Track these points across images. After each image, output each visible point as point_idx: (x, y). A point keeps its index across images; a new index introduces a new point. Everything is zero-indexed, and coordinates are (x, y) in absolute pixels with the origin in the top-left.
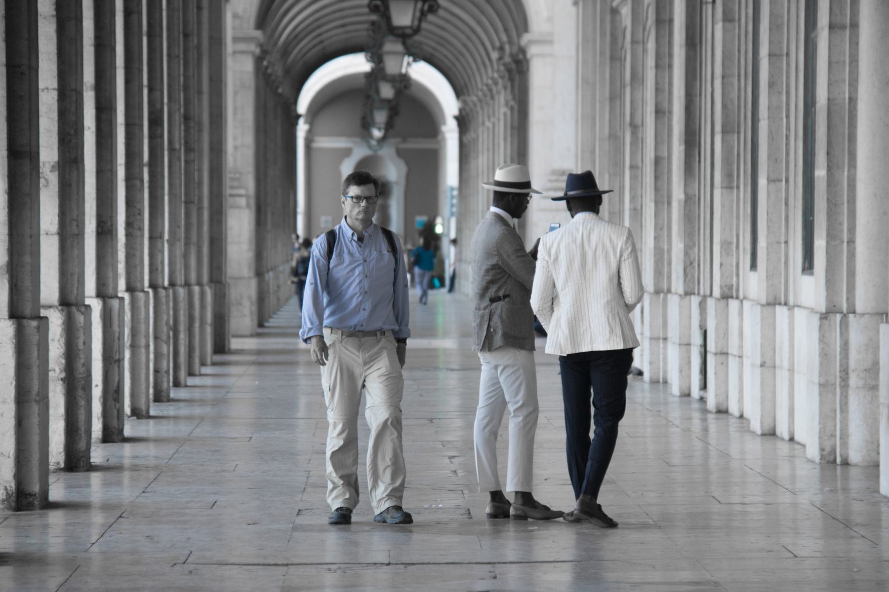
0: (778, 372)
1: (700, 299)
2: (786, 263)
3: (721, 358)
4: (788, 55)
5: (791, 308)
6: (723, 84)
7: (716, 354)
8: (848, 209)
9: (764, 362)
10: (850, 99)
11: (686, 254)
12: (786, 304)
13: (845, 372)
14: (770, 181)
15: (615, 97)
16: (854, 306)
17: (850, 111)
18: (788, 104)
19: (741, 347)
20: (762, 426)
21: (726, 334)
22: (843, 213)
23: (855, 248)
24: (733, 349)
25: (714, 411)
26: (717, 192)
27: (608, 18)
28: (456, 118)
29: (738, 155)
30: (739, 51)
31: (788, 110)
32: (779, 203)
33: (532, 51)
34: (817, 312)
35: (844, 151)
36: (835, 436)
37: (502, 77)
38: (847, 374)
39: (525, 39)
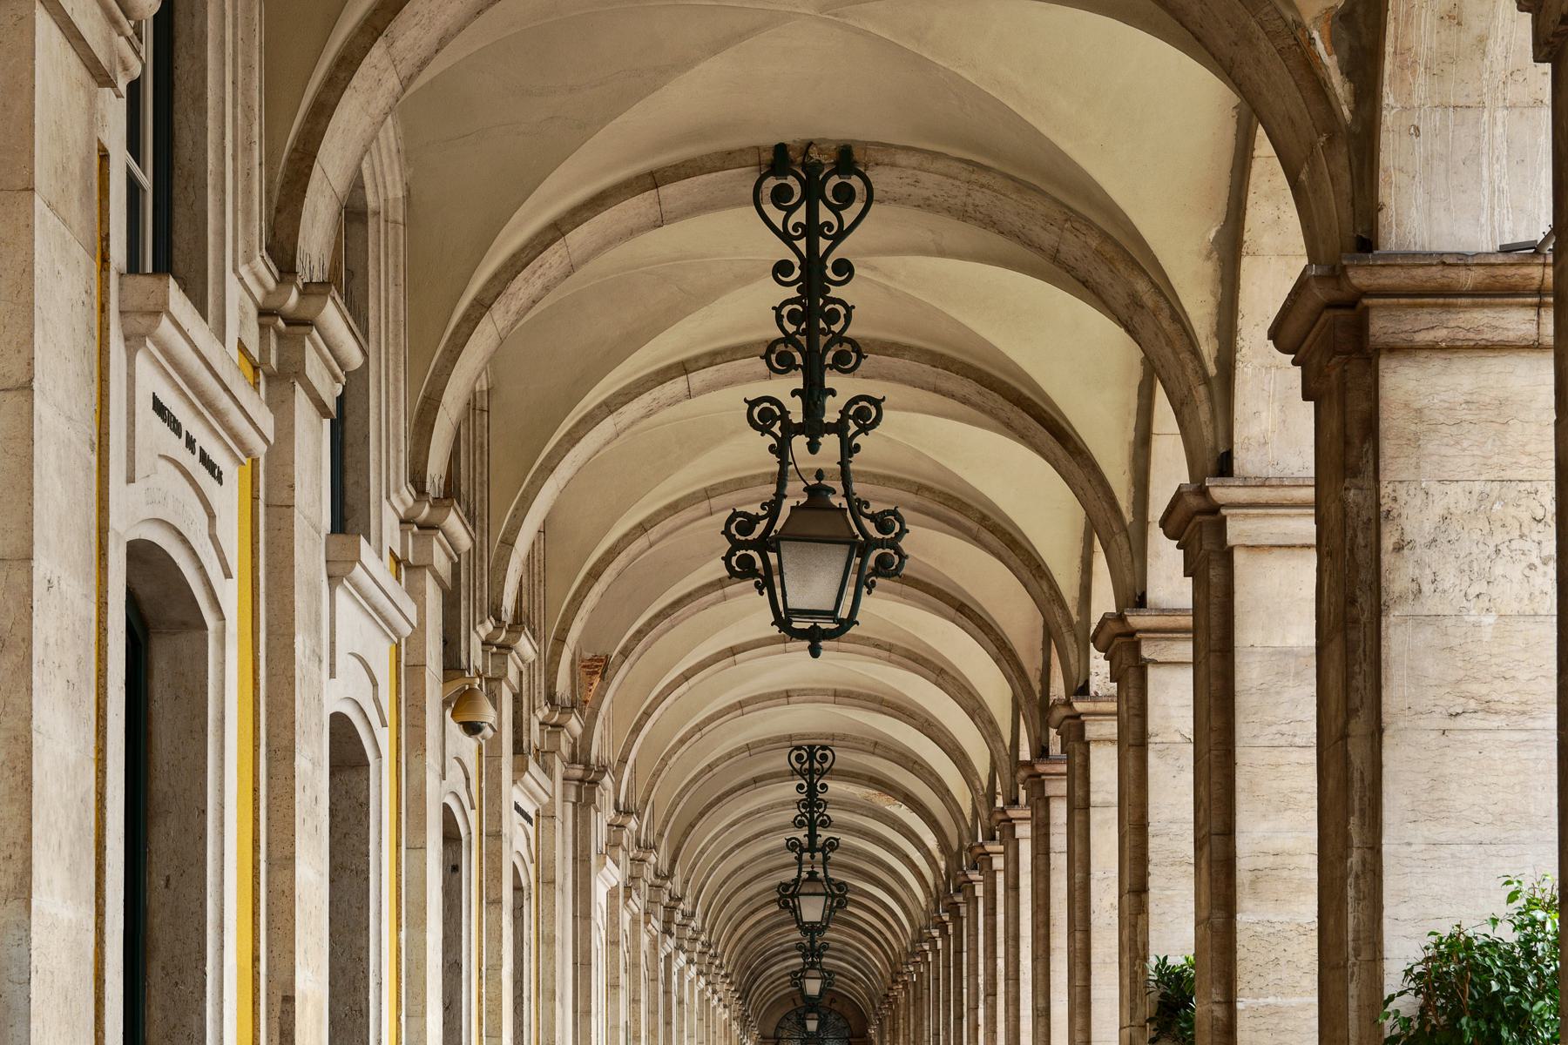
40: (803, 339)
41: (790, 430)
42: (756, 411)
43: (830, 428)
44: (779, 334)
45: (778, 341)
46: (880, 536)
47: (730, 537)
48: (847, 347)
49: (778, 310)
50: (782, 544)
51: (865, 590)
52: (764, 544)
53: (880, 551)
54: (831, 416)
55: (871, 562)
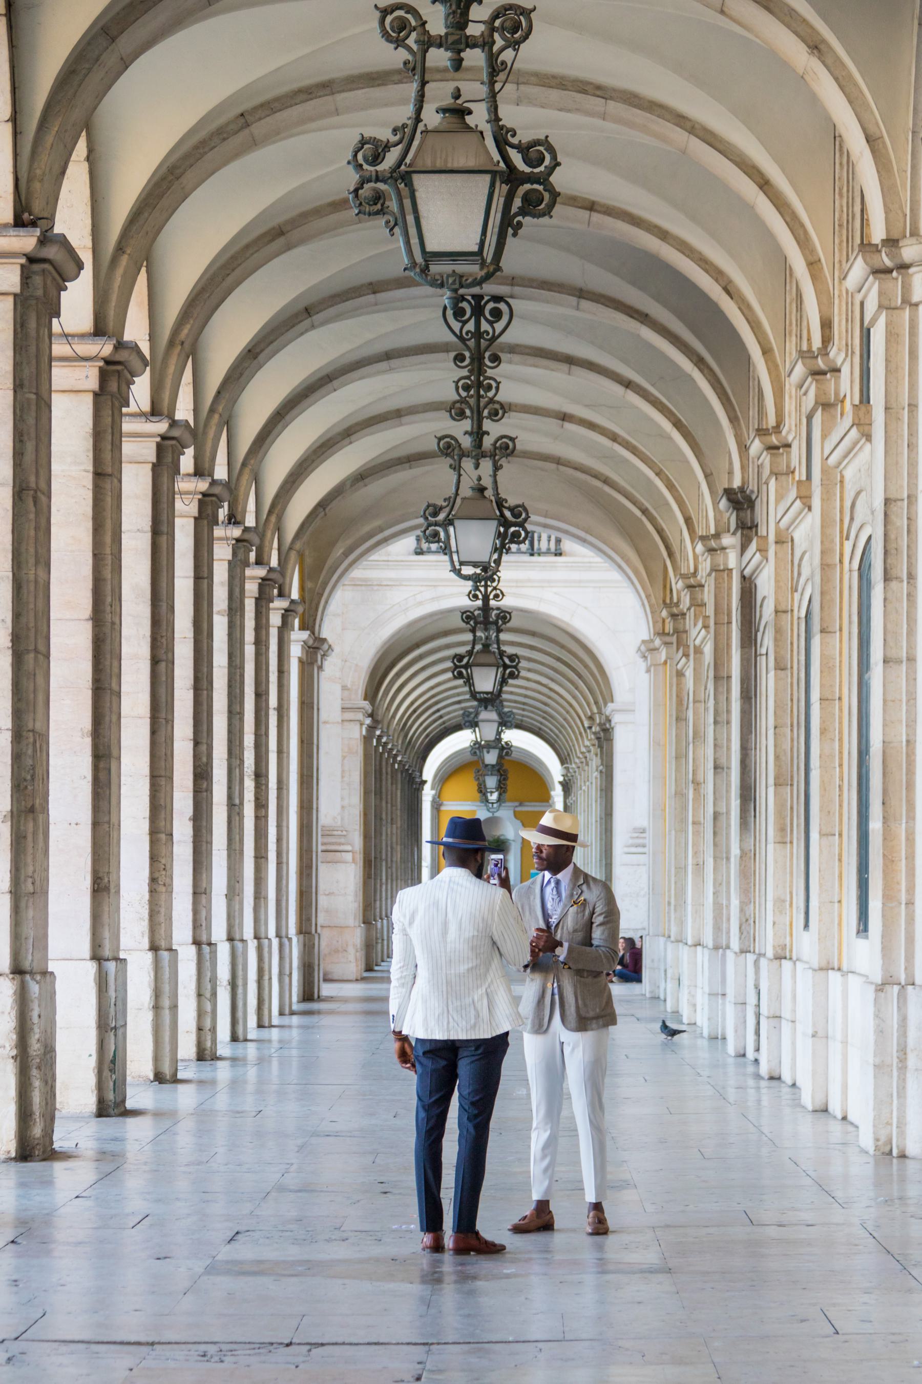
0: (830, 1042)
1: (755, 957)
2: (840, 924)
3: (774, 1022)
4: (840, 699)
5: (845, 974)
6: (775, 734)
7: (768, 1018)
8: (907, 866)
9: (816, 1032)
10: (908, 741)
11: (742, 910)
12: (839, 969)
13: (903, 1051)
14: (822, 835)
15: (680, 756)
16: (913, 976)
17: (908, 755)
18: (841, 753)
19: (794, 1011)
20: (813, 1103)
21: (779, 997)
22: (901, 871)
23: (914, 911)
24: (786, 1014)
25: (767, 1077)
26: (771, 847)
27: (675, 679)
28: (560, 783)
29: (792, 808)
30: (792, 700)
31: (841, 759)
32: (833, 858)
33: (616, 719)
34: (872, 983)
35: (901, 800)
36: (891, 1124)
37: (594, 745)
38: (905, 1054)
39: (610, 706)
40: (472, 401)
41: (428, 42)
42: (389, 19)
43: (492, 623)
44: (458, 398)
45: (455, 402)
46: (528, 170)
47: (426, 519)
48: (497, 406)
49: (457, 383)
50: (415, 177)
51: (510, 231)
52: (466, 667)
53: (528, 186)
54: (474, 30)
55: (517, 203)
